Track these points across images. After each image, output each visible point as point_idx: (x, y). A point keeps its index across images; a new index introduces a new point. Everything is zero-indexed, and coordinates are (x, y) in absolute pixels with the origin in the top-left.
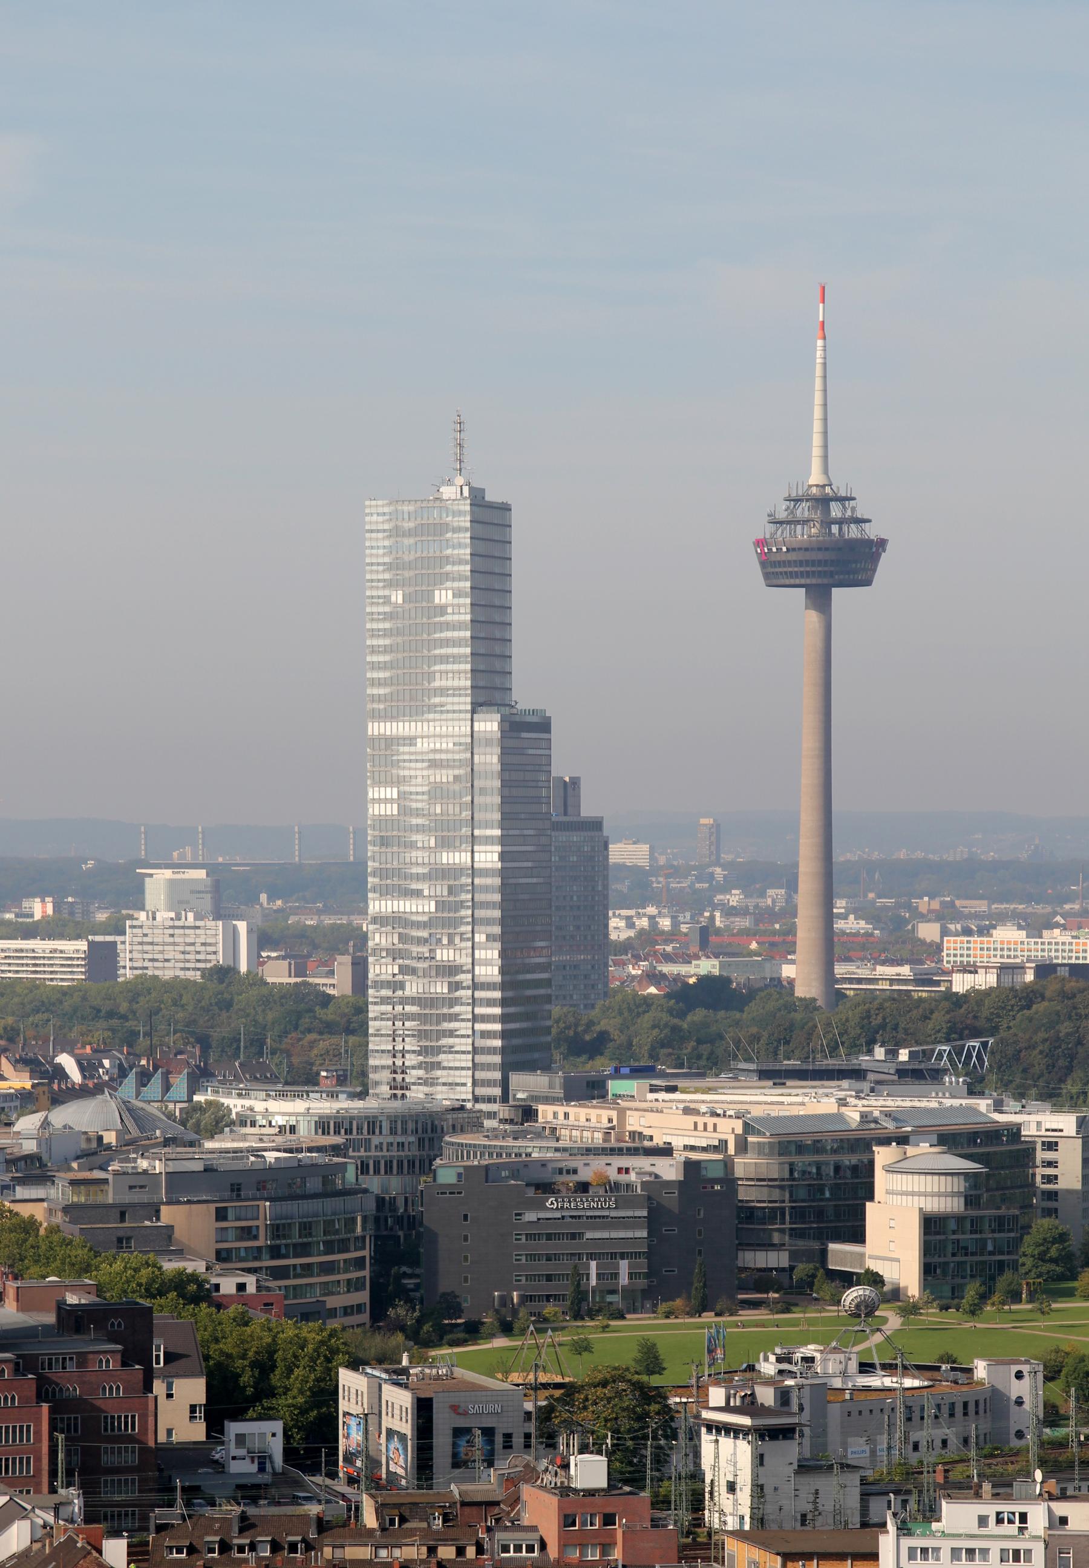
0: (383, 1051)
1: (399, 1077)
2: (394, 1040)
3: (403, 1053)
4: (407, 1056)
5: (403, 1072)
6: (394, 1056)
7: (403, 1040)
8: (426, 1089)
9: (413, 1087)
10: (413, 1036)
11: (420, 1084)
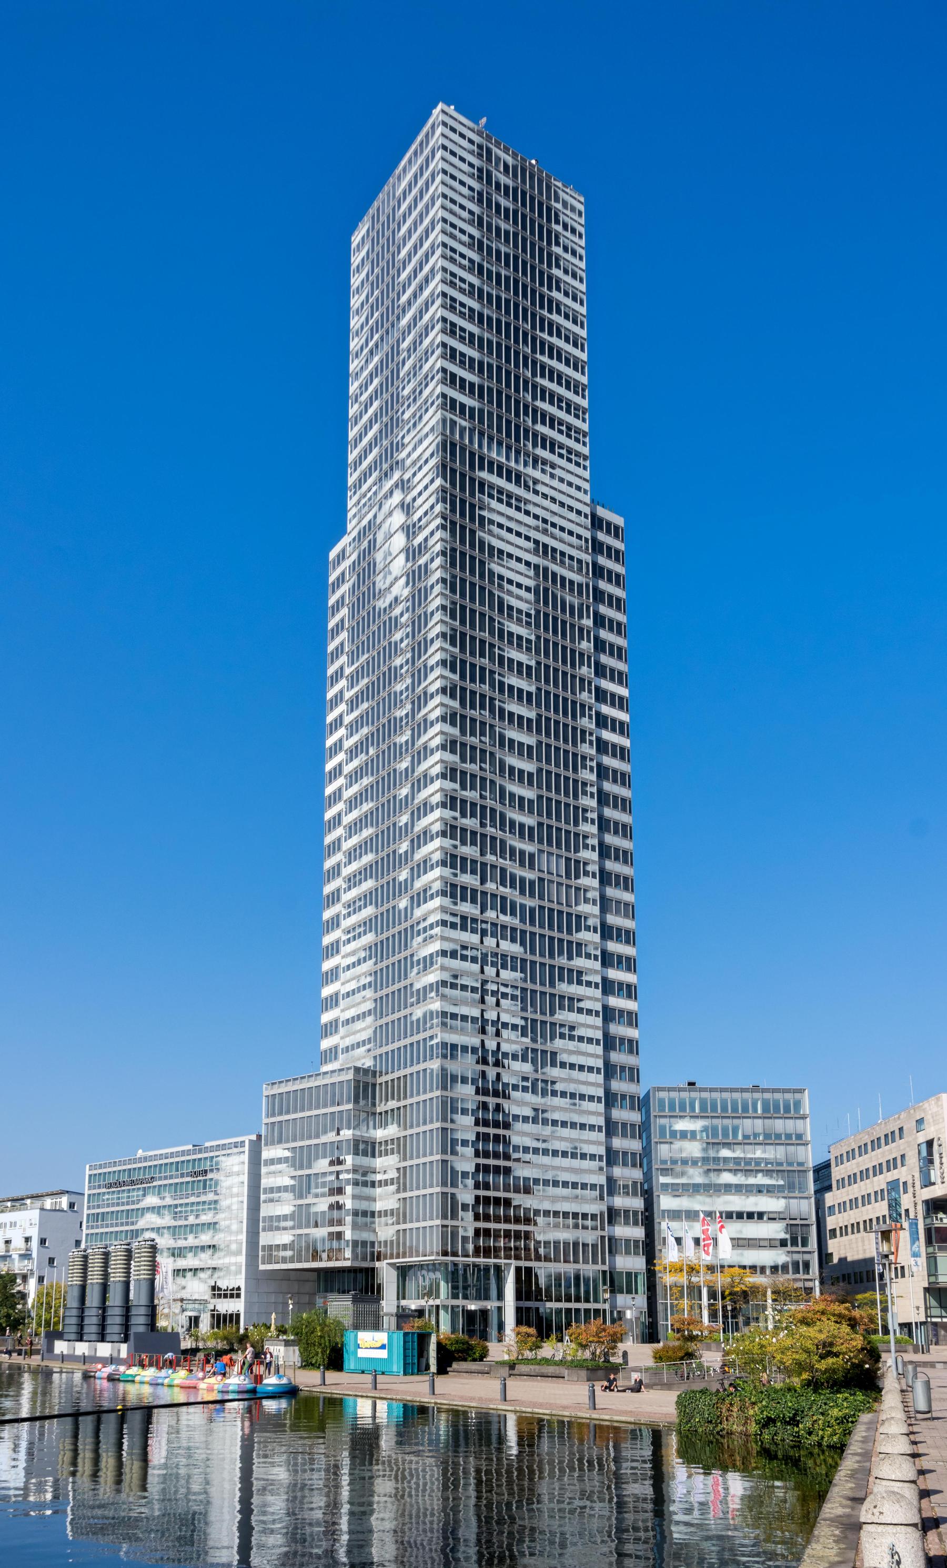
0: (464, 1018)
1: (491, 1073)
2: (483, 1001)
3: (500, 1026)
4: (505, 1033)
5: (497, 1064)
6: (483, 1031)
7: (498, 1004)
8: (537, 1100)
9: (515, 1095)
10: (514, 998)
11: (525, 1089)
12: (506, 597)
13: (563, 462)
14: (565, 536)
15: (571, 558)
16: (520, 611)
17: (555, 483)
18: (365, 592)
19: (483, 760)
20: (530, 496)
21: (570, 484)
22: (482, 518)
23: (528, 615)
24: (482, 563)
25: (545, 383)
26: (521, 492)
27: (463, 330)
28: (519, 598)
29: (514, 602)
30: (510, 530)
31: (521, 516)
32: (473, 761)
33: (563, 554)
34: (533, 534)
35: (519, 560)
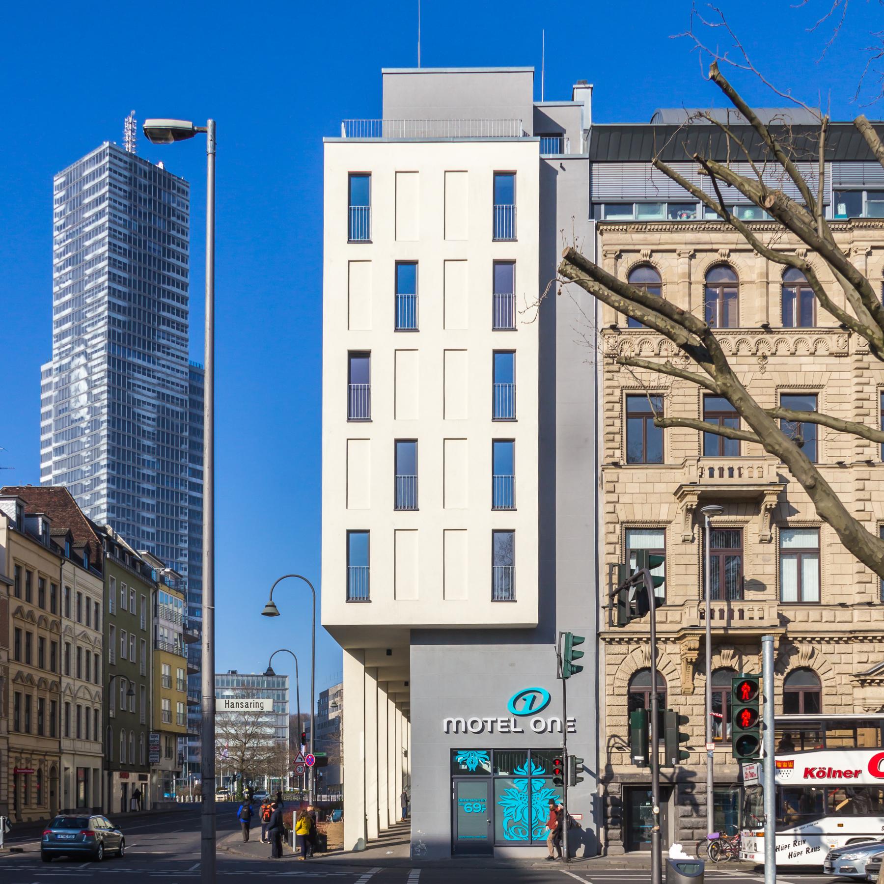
12: (142, 426)
13: (174, 345)
14: (174, 387)
15: (177, 399)
16: (149, 433)
17: (170, 358)
18: (63, 410)
19: (128, 515)
20: (156, 367)
21: (178, 357)
22: (129, 383)
23: (154, 434)
24: (129, 409)
25: (166, 300)
26: (151, 366)
27: (120, 277)
28: (148, 425)
29: (146, 428)
30: (144, 388)
31: (150, 379)
32: (123, 516)
33: (173, 397)
34: (158, 389)
35: (149, 404)
